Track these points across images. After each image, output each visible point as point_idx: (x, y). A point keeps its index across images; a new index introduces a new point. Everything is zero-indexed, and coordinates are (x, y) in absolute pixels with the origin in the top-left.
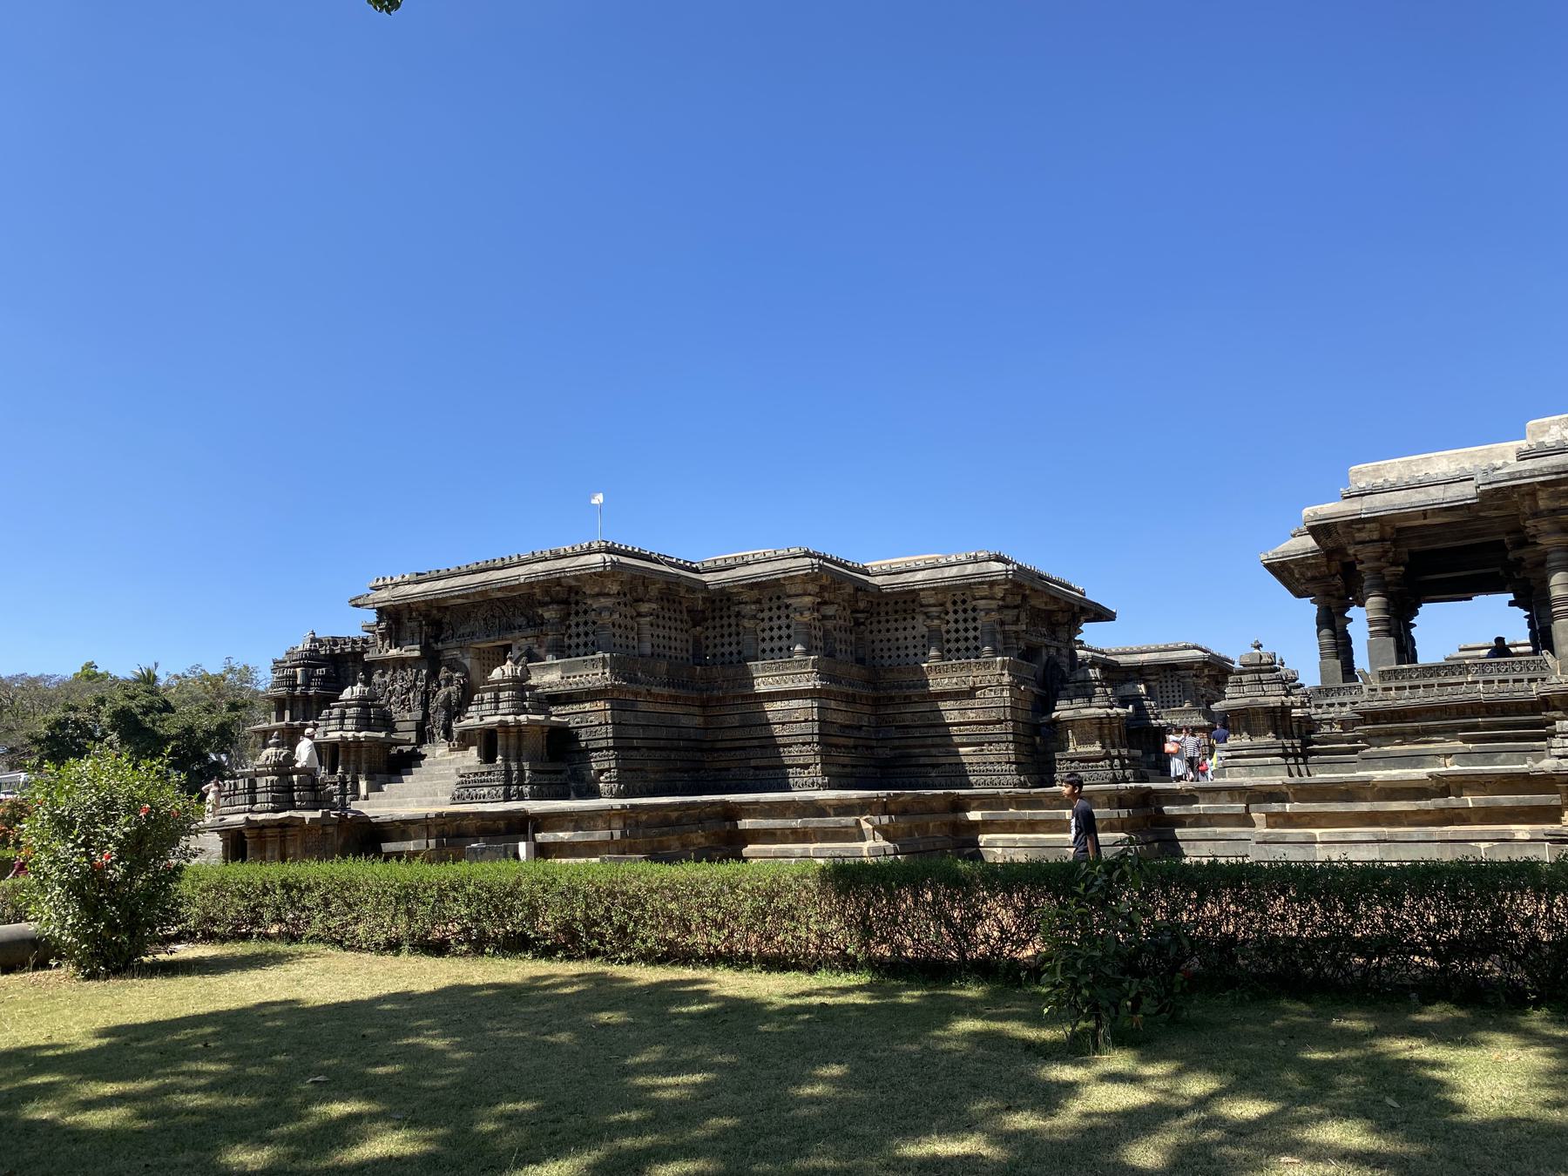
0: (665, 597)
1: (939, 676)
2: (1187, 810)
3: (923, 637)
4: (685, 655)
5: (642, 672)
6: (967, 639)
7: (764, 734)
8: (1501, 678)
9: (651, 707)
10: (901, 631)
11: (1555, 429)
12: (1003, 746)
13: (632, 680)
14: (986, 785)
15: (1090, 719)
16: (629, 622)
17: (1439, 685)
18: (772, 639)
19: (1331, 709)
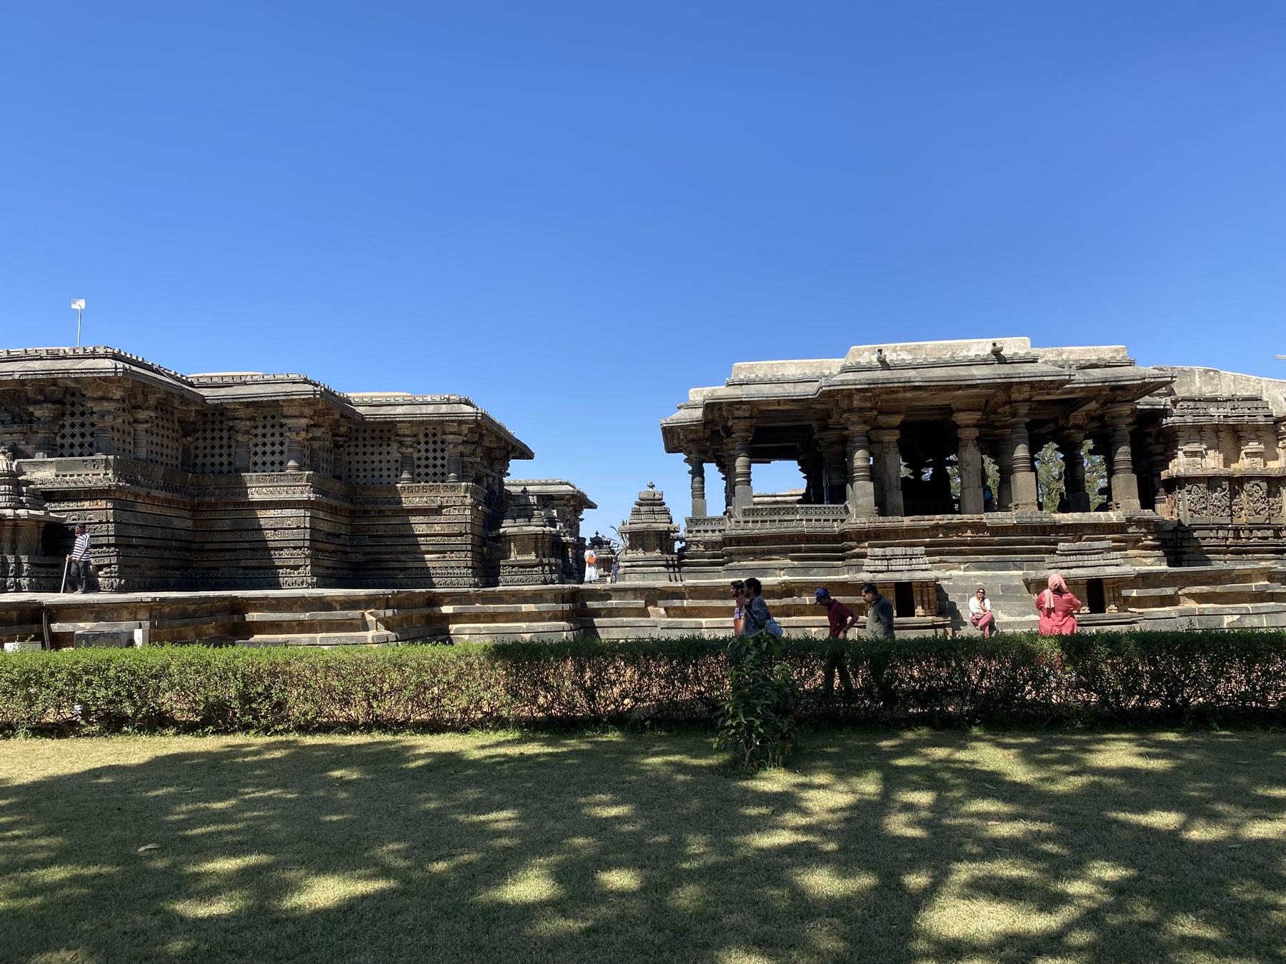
0: (159, 406)
1: (411, 495)
2: (604, 605)
3: (396, 461)
4: (174, 462)
5: (142, 475)
6: (435, 466)
7: (256, 537)
8: (817, 518)
9: (149, 509)
10: (376, 455)
11: (866, 354)
12: (463, 554)
13: (134, 482)
14: (446, 585)
15: (529, 535)
16: (126, 427)
17: (780, 521)
18: (264, 453)
19: (698, 534)
